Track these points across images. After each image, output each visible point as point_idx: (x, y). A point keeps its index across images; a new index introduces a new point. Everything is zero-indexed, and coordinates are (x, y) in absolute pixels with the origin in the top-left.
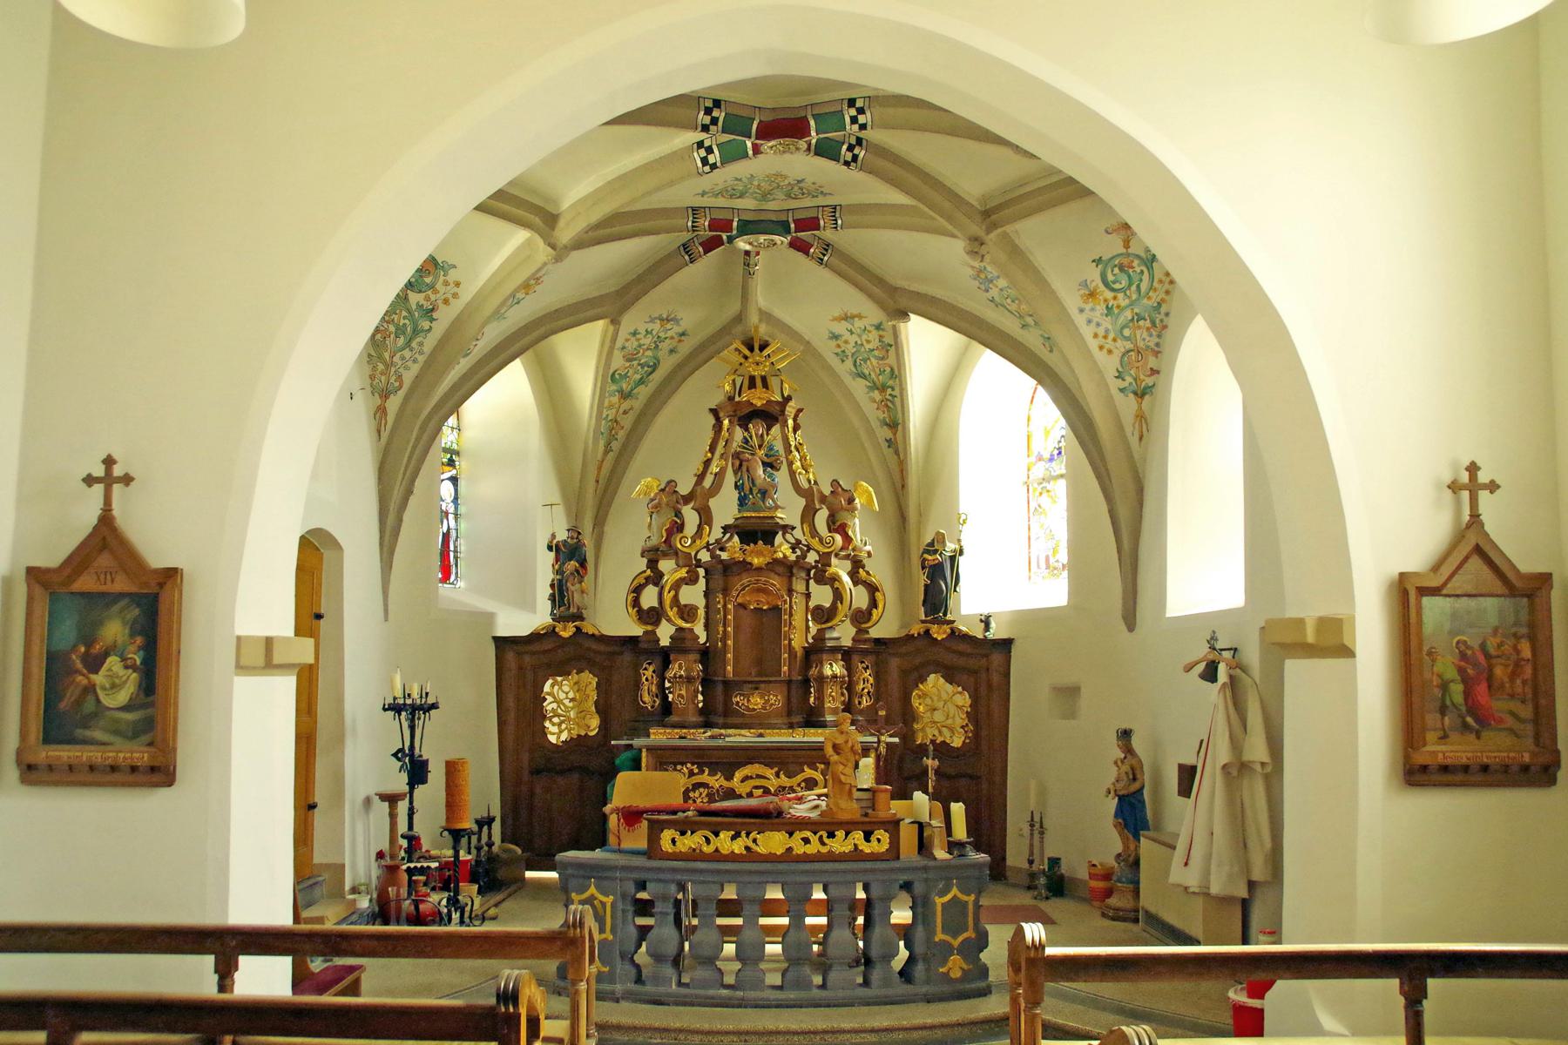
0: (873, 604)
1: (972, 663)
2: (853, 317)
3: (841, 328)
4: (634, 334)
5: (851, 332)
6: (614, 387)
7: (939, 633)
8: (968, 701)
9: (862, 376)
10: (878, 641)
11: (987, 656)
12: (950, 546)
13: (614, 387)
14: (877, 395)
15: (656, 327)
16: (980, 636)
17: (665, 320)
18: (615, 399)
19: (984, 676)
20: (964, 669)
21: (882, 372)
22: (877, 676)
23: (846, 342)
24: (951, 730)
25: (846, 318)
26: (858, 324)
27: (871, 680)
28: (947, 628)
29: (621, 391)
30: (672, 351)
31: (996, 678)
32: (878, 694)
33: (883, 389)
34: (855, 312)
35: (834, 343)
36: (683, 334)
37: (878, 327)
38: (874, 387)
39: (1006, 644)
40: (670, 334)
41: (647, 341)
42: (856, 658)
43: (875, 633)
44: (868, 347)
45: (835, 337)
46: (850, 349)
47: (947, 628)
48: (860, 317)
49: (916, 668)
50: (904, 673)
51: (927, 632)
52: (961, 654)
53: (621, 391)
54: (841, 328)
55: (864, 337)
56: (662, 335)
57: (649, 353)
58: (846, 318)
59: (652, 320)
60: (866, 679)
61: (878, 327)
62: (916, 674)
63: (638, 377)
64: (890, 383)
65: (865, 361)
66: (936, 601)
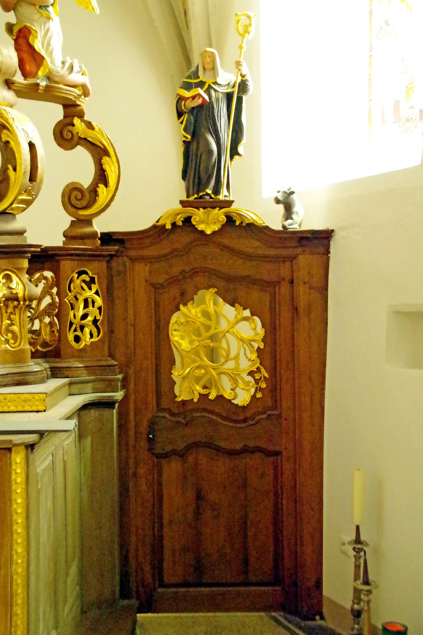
0: (101, 177)
1: (266, 272)
7: (208, 222)
8: (261, 331)
10: (107, 238)
11: (293, 258)
12: (226, 78)
16: (277, 226)
19: (285, 289)
20: (253, 282)
22: (109, 294)
24: (234, 379)
27: (99, 301)
28: (219, 215)
31: (303, 294)
32: (109, 324)
39: (320, 240)
42: (66, 265)
43: (100, 225)
47: (219, 215)
49: (174, 281)
50: (157, 287)
51: (188, 220)
52: (249, 257)
60: (87, 299)
62: (175, 291)
66: (201, 171)
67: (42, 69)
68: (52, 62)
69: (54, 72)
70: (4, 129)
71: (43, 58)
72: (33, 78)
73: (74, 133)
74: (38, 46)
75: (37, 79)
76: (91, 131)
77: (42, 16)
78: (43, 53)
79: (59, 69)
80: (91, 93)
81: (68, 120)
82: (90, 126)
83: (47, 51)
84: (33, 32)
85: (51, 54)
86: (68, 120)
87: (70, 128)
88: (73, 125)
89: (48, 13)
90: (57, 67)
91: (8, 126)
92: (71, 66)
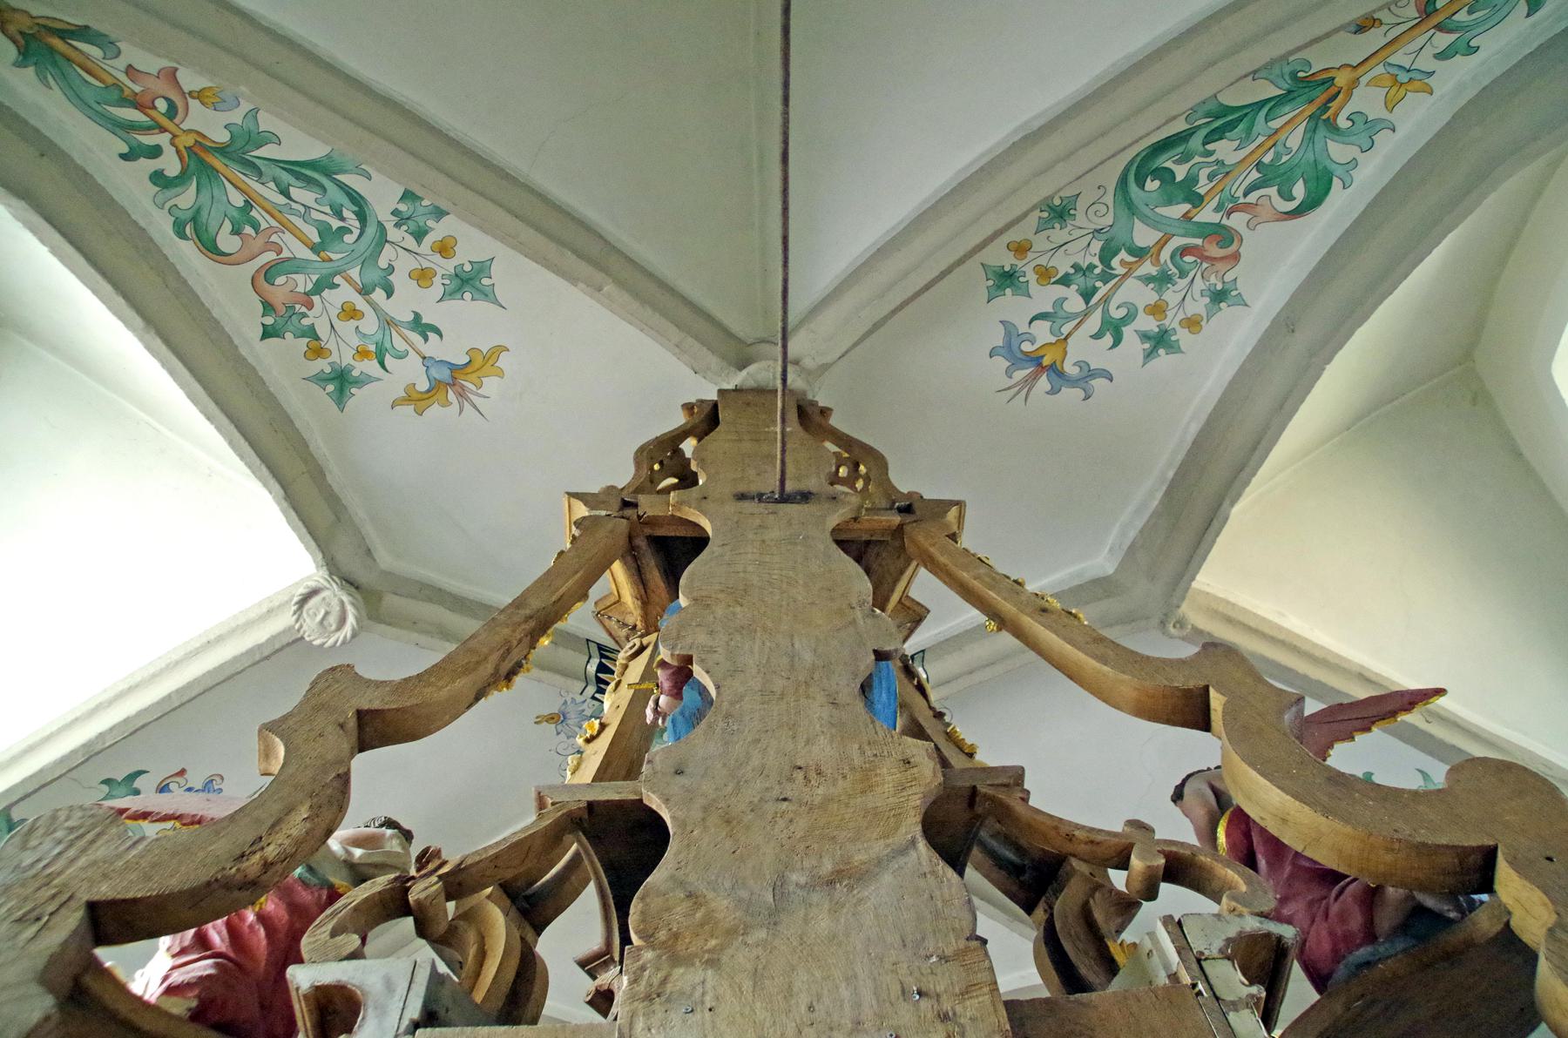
2: (436, 387)
3: (464, 327)
4: (1160, 341)
5: (422, 327)
6: (1338, 151)
9: (302, 171)
13: (1338, 151)
14: (213, 125)
15: (1084, 349)
17: (1045, 366)
18: (1366, 100)
21: (242, 221)
23: (423, 277)
25: (452, 380)
26: (409, 372)
29: (1322, 121)
30: (1060, 213)
33: (200, 161)
34: (435, 410)
35: (464, 256)
36: (1006, 279)
37: (342, 381)
38: (241, 150)
40: (1044, 297)
41: (1134, 292)
44: (344, 293)
45: (467, 282)
46: (400, 259)
48: (417, 400)
53: (1322, 121)
54: (464, 327)
55: (370, 324)
56: (1075, 304)
57: (1144, 236)
58: (452, 380)
59: (1089, 374)
61: (342, 381)
63: (1225, 150)
64: (186, 198)
65: (329, 236)
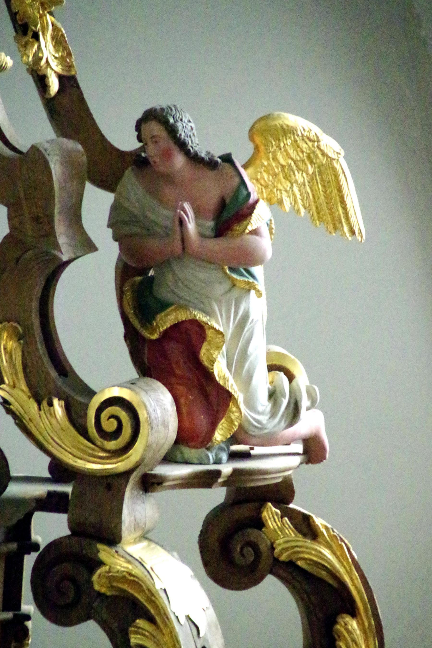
67: (223, 424)
68: (250, 403)
69: (251, 428)
70: (140, 617)
71: (229, 396)
72: (196, 447)
73: (263, 547)
74: (220, 370)
75: (208, 449)
76: (309, 543)
77: (234, 285)
78: (232, 386)
79: (264, 419)
80: (327, 456)
81: (245, 511)
82: (305, 526)
83: (237, 375)
84: (209, 333)
85: (247, 382)
86: (245, 511)
87: (252, 534)
88: (260, 524)
89: (251, 280)
90: (258, 413)
91: (152, 611)
92: (292, 406)
